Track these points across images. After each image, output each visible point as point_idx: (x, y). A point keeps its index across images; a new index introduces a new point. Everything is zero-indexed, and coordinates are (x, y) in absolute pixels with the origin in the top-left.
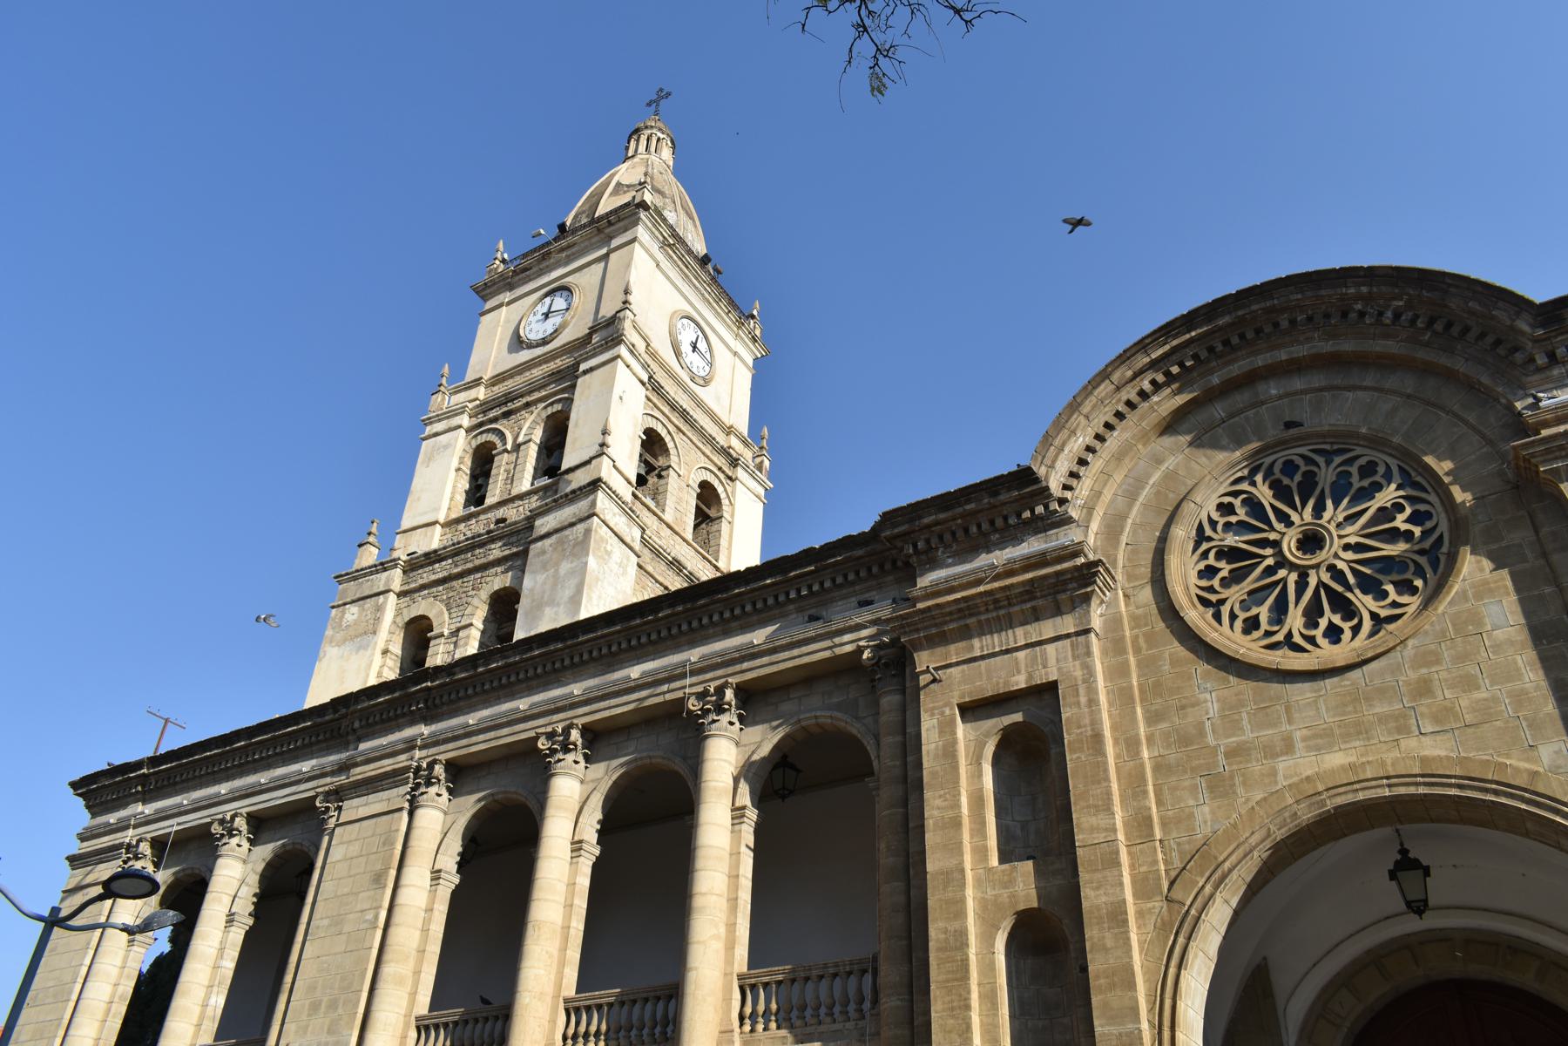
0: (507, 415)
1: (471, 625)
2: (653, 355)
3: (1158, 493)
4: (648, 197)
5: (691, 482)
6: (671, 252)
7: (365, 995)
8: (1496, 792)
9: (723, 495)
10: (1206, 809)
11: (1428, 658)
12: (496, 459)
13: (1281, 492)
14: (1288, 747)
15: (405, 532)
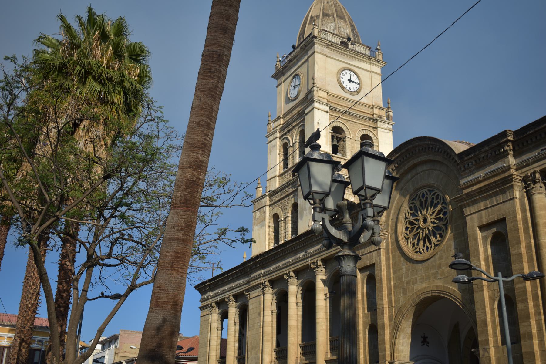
0: (289, 131)
1: (288, 216)
2: (332, 95)
3: (398, 203)
4: (316, 33)
5: (356, 139)
6: (331, 47)
7: (261, 345)
8: (448, 295)
9: (372, 137)
10: (402, 298)
11: (441, 258)
12: (289, 149)
13: (421, 204)
14: (416, 282)
15: (269, 180)
